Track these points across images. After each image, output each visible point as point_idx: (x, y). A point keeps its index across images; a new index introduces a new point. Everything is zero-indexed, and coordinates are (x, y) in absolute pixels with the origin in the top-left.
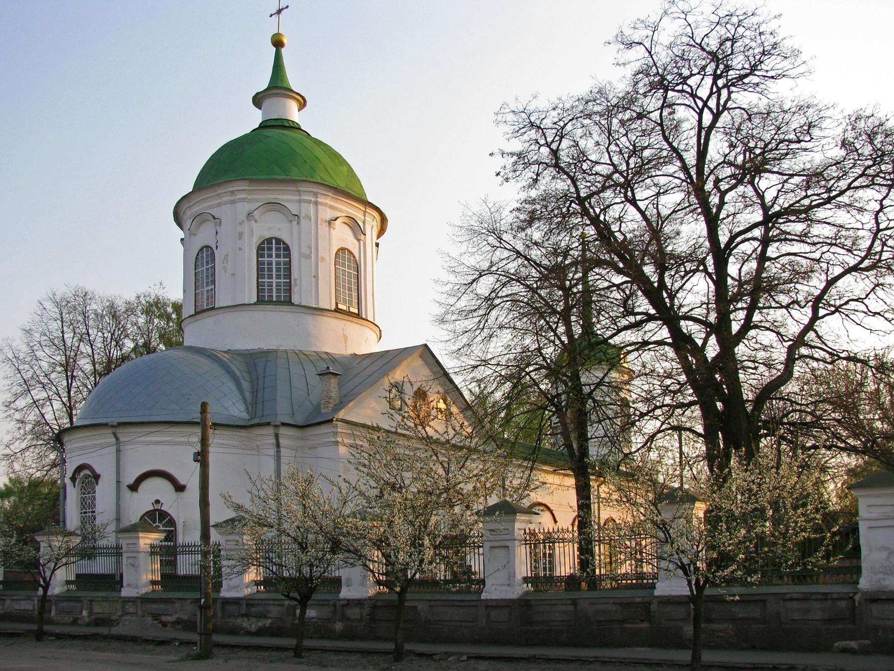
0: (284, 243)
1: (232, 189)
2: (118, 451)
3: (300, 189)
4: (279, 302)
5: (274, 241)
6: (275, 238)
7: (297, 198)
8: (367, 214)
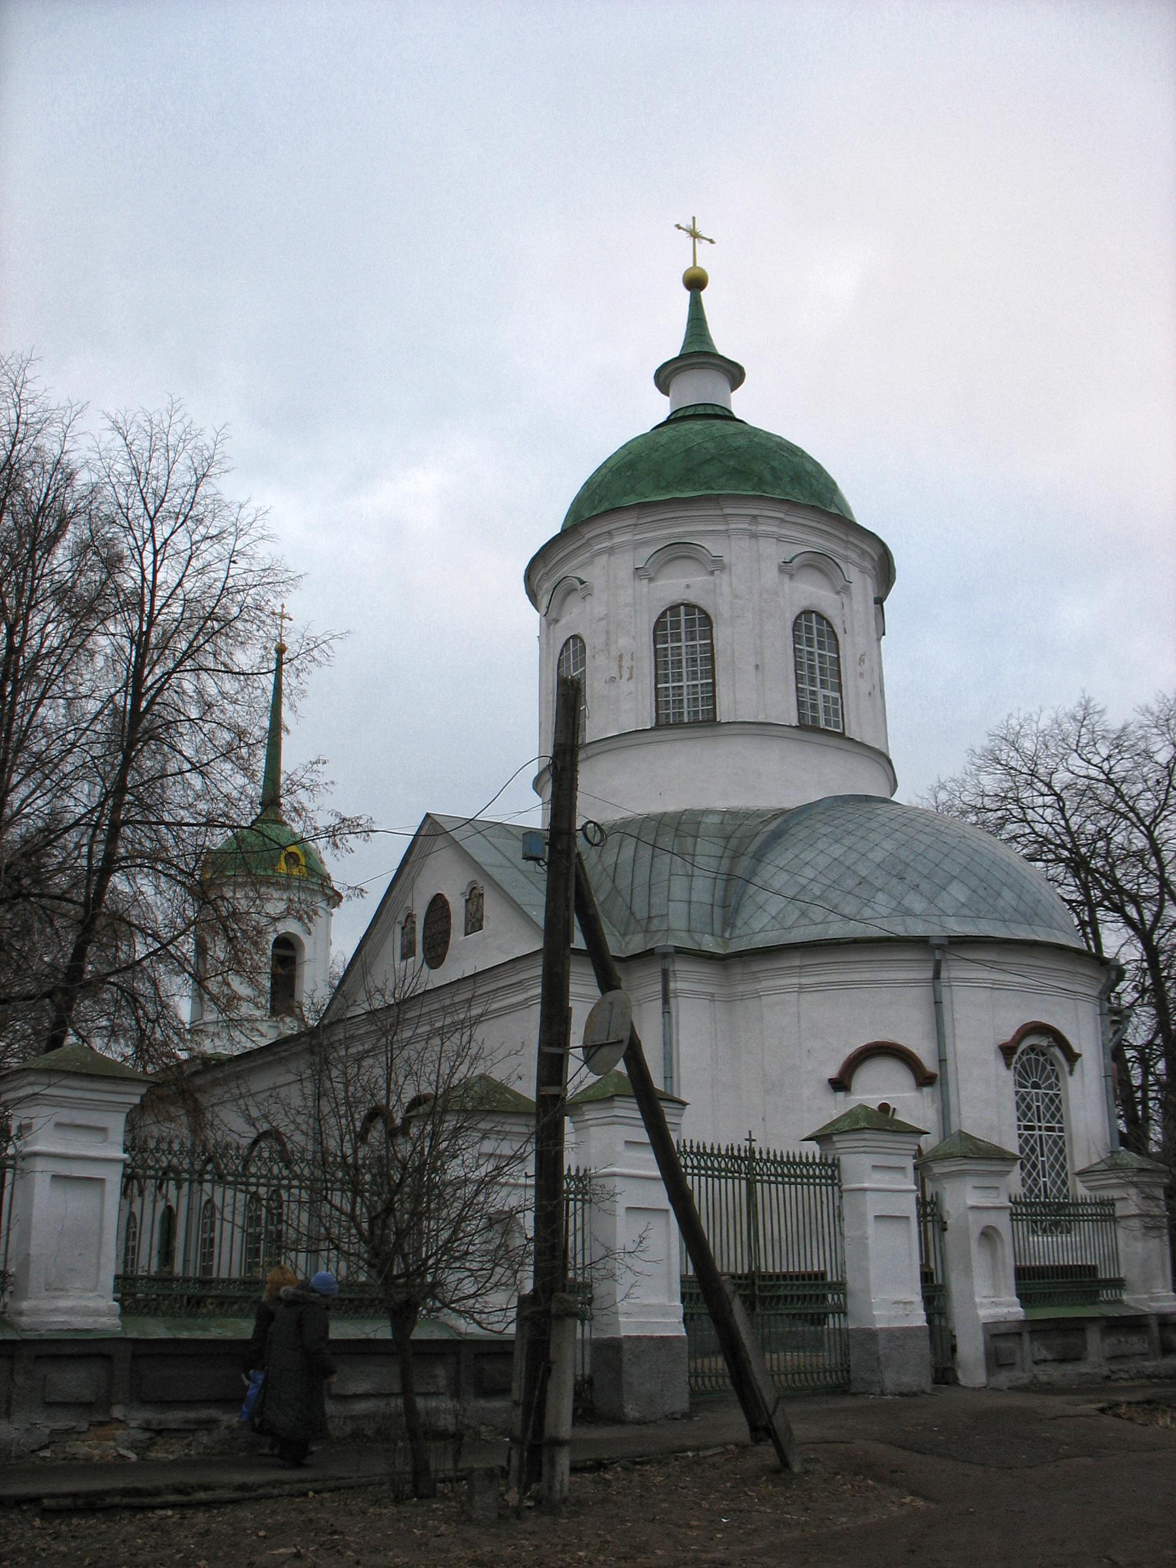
4: (695, 724)
6: (682, 604)
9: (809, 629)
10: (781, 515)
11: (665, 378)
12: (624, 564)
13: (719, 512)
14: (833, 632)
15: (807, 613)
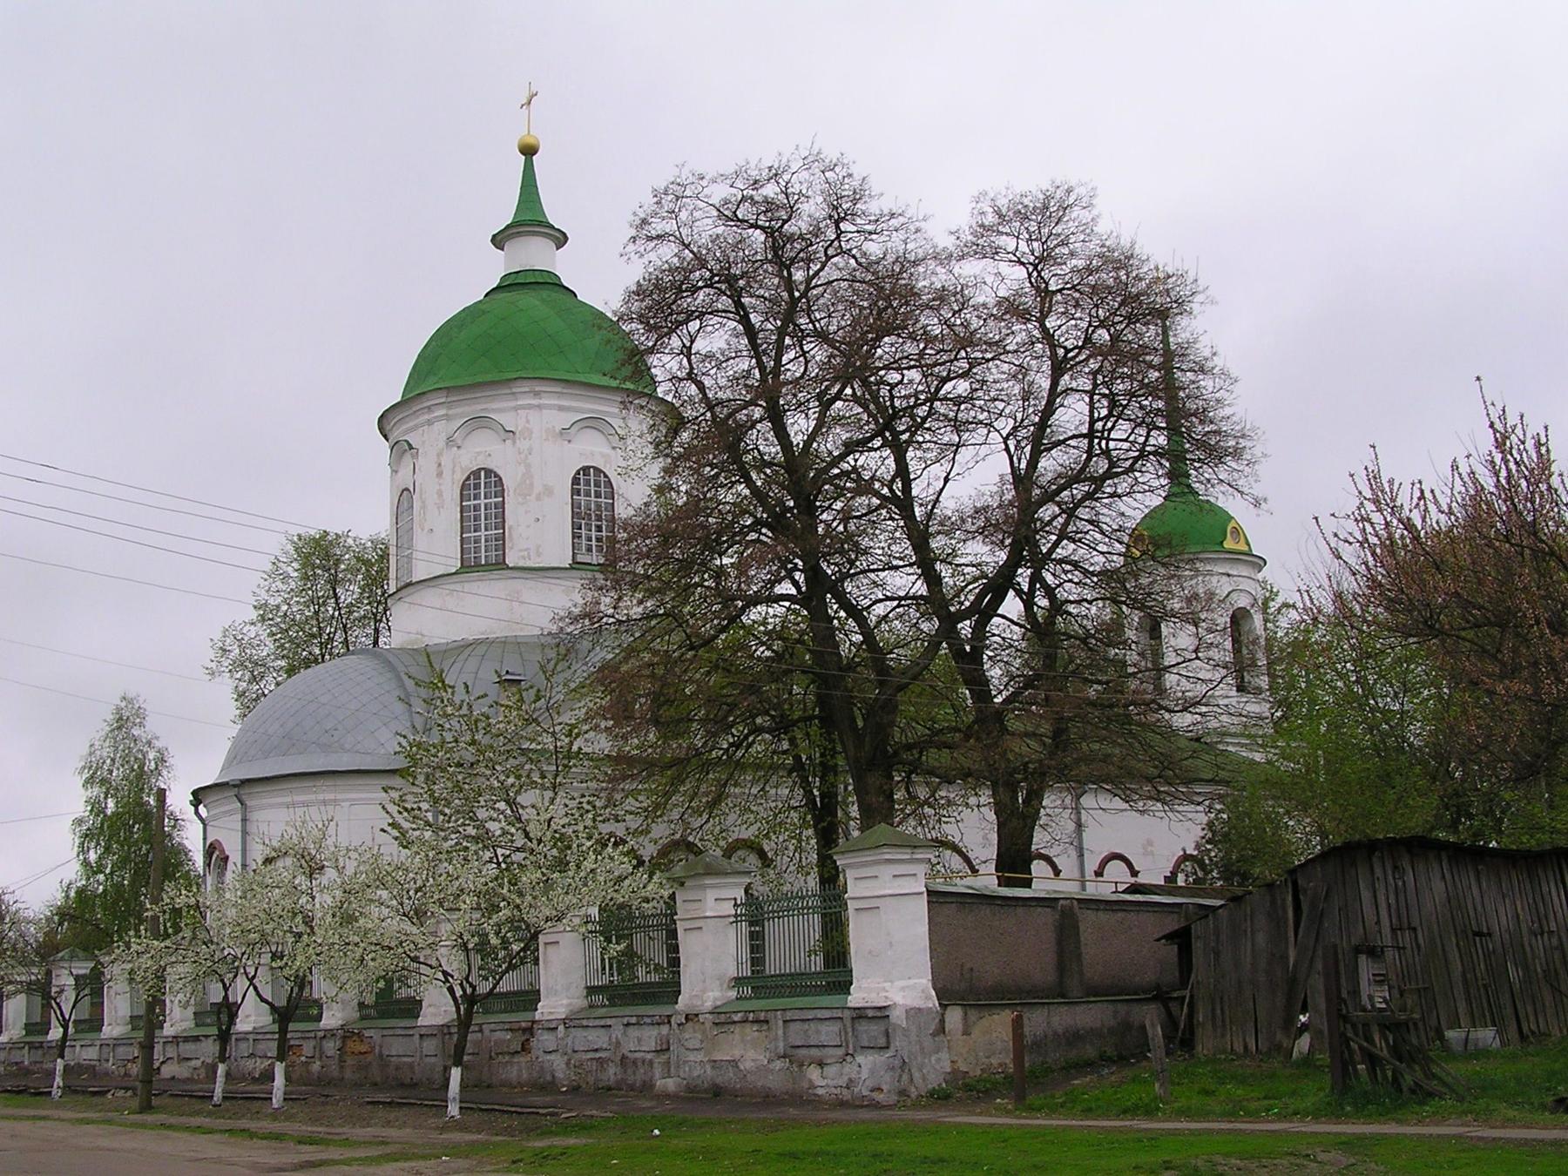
0: (496, 475)
3: (514, 390)
5: (483, 473)
9: (588, 483)
10: (559, 390)
11: (499, 241)
12: (441, 430)
13: (508, 391)
14: (610, 481)
15: (586, 470)
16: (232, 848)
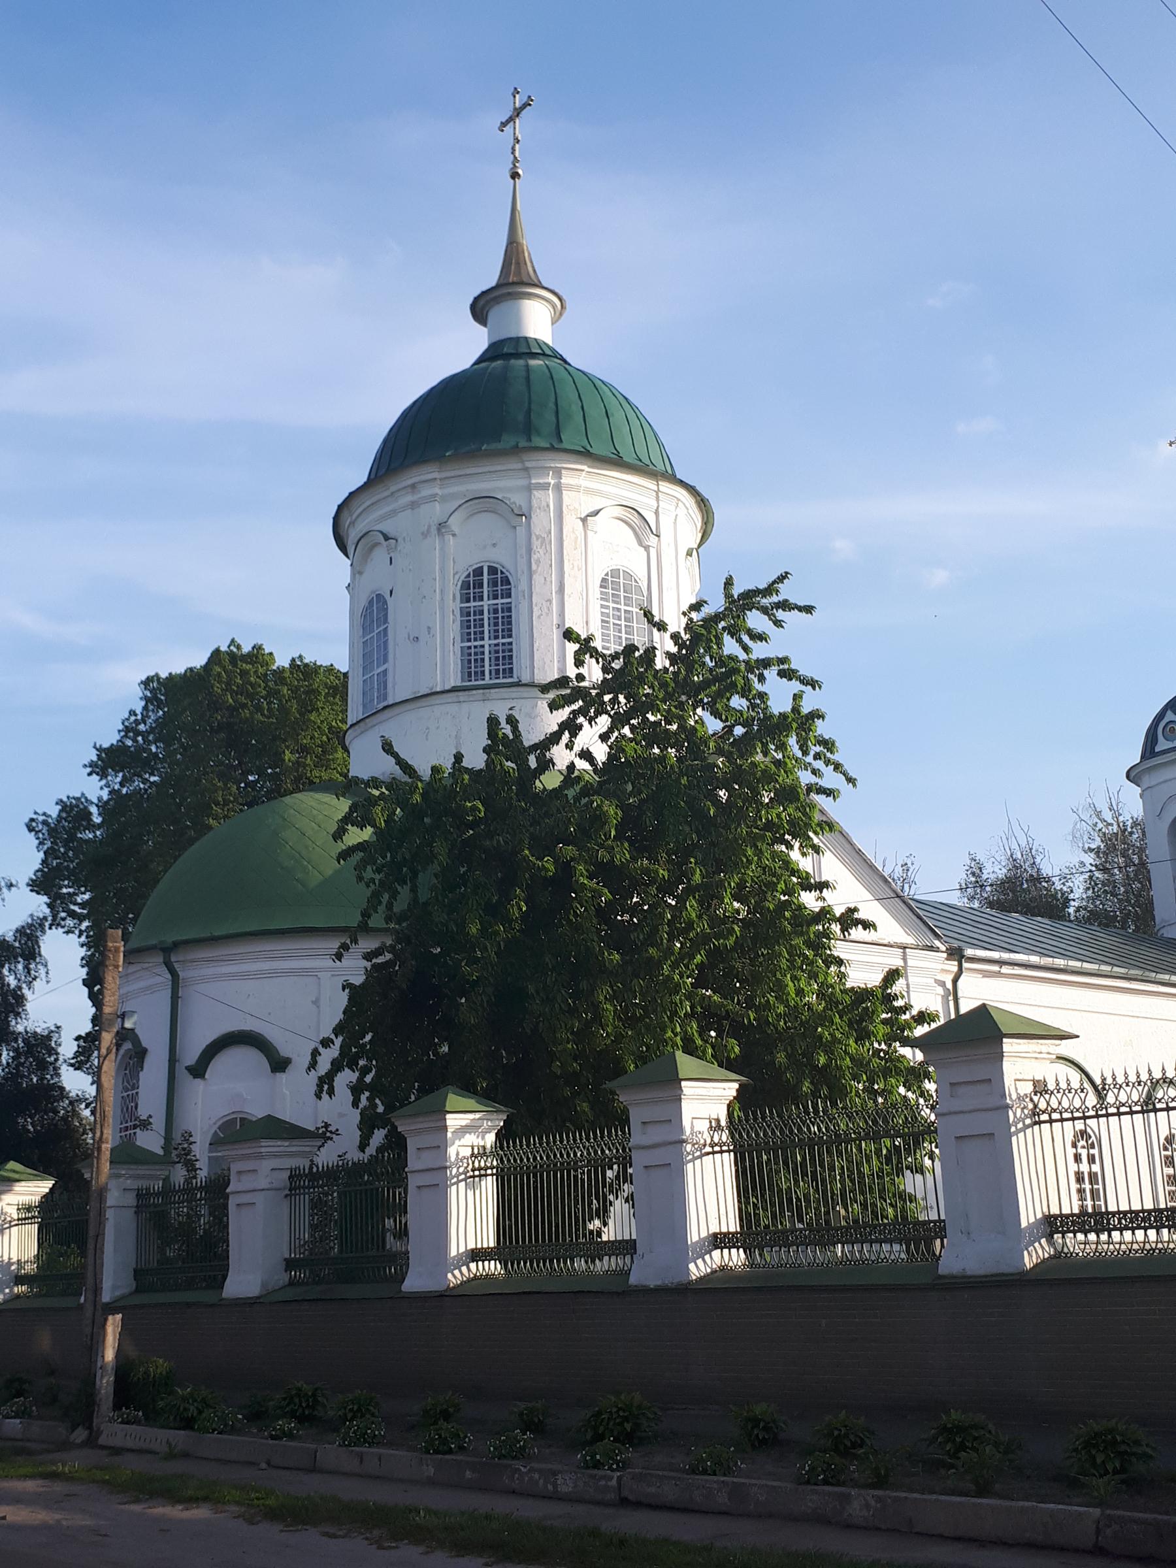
1: (410, 482)
2: (175, 998)
3: (528, 464)
7: (522, 482)
8: (660, 494)
13: (520, 466)
16: (155, 1040)
